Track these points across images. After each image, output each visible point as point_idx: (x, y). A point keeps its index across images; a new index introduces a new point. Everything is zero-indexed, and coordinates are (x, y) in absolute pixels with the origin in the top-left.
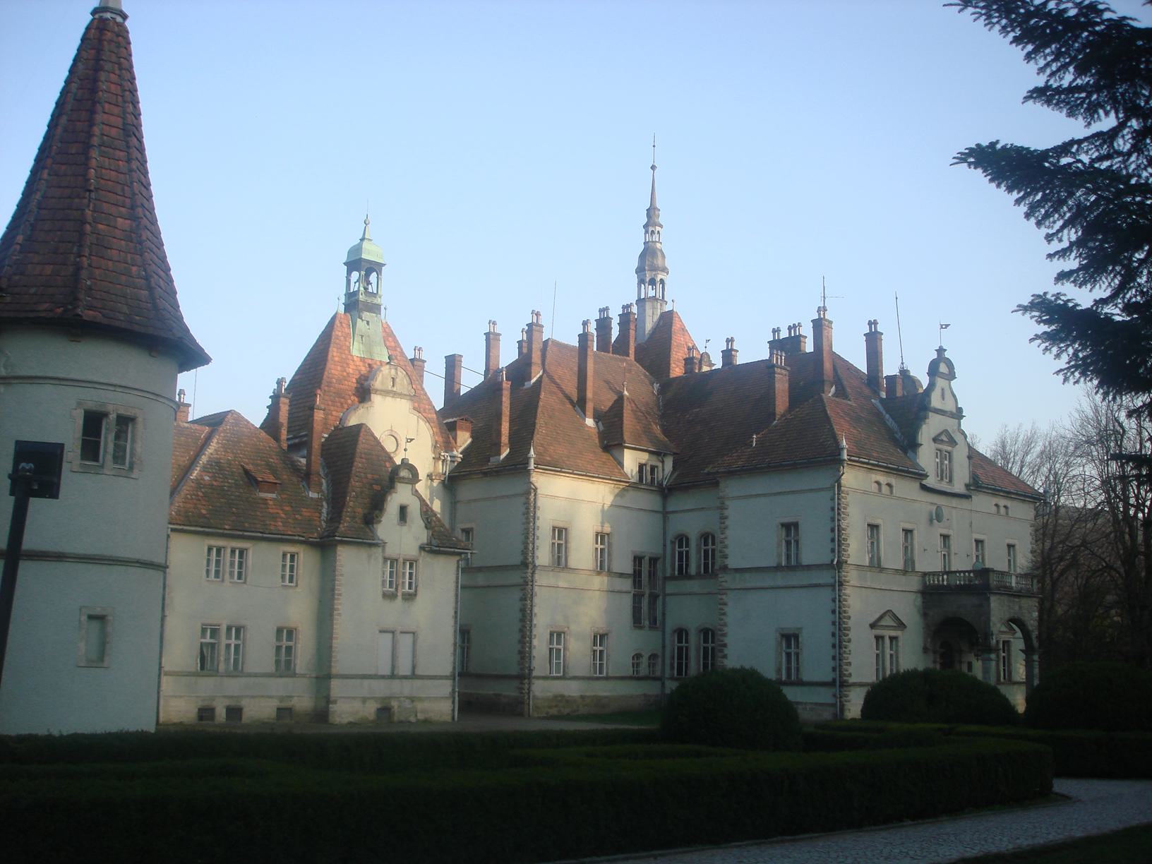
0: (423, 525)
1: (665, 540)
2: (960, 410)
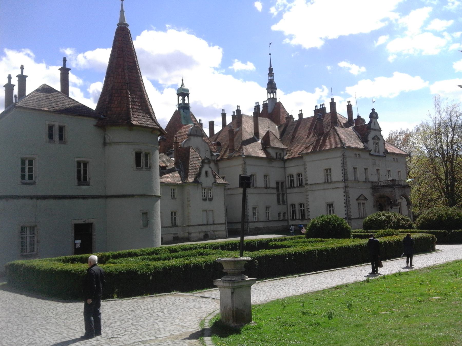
0: (212, 176)
1: (285, 176)
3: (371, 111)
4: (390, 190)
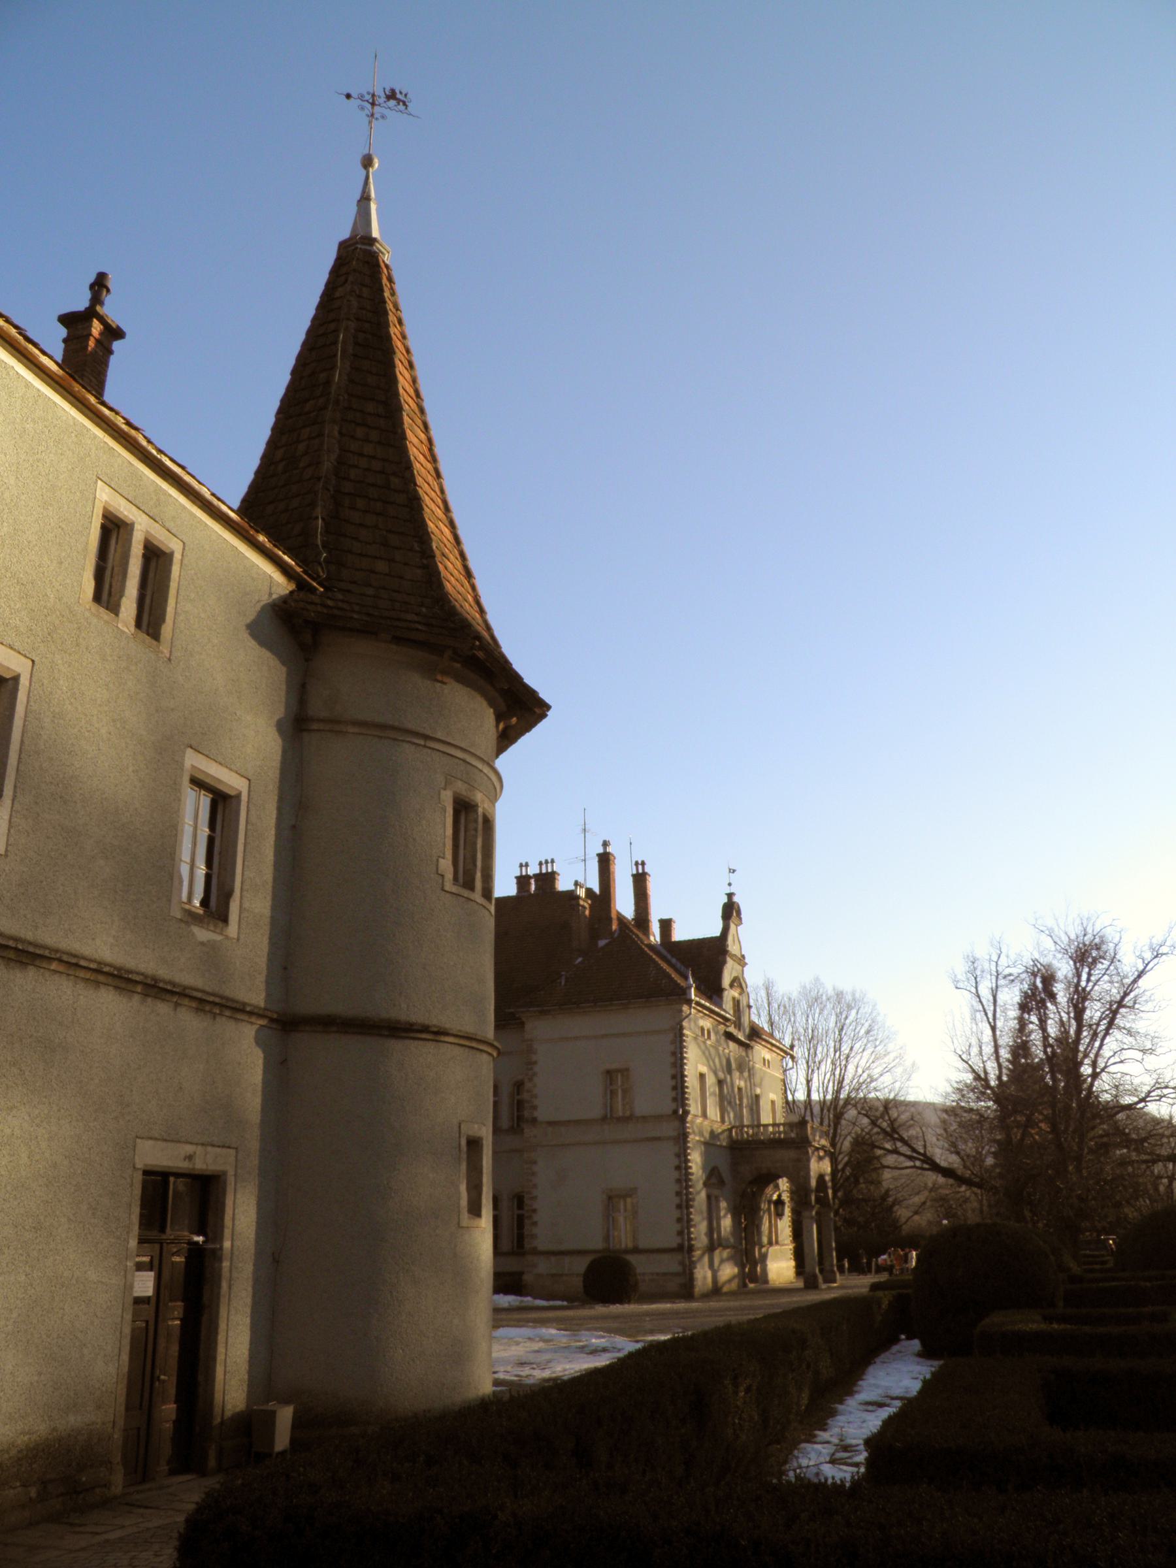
2: (743, 956)
3: (725, 900)
4: (792, 1154)
